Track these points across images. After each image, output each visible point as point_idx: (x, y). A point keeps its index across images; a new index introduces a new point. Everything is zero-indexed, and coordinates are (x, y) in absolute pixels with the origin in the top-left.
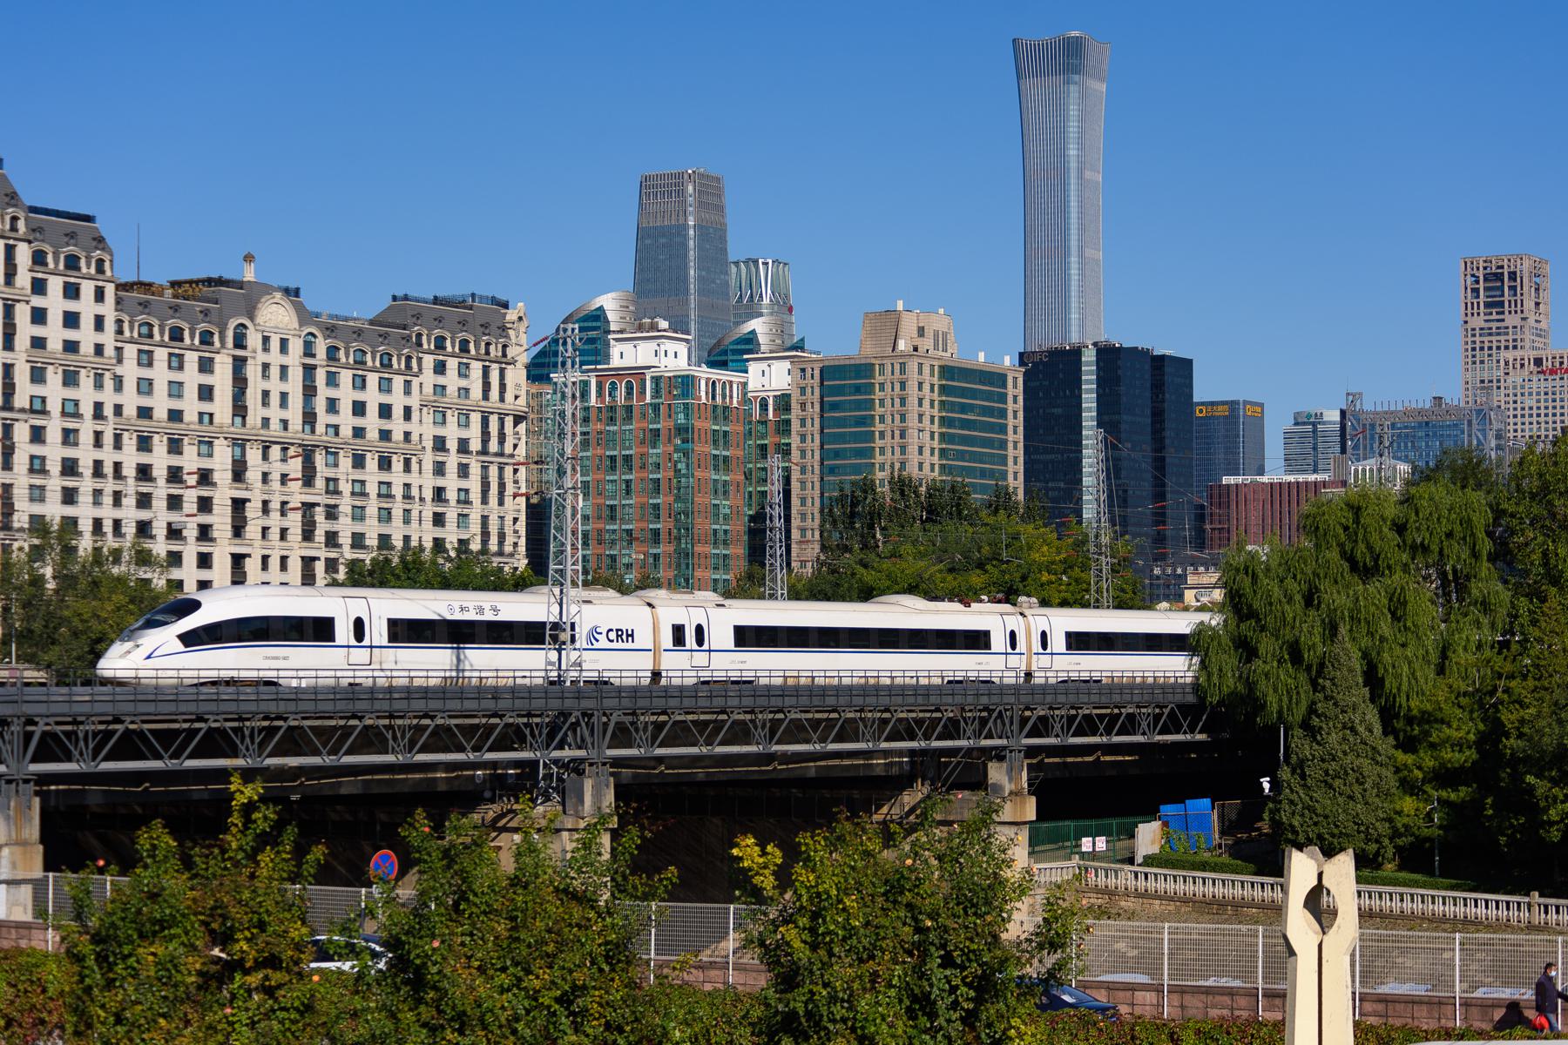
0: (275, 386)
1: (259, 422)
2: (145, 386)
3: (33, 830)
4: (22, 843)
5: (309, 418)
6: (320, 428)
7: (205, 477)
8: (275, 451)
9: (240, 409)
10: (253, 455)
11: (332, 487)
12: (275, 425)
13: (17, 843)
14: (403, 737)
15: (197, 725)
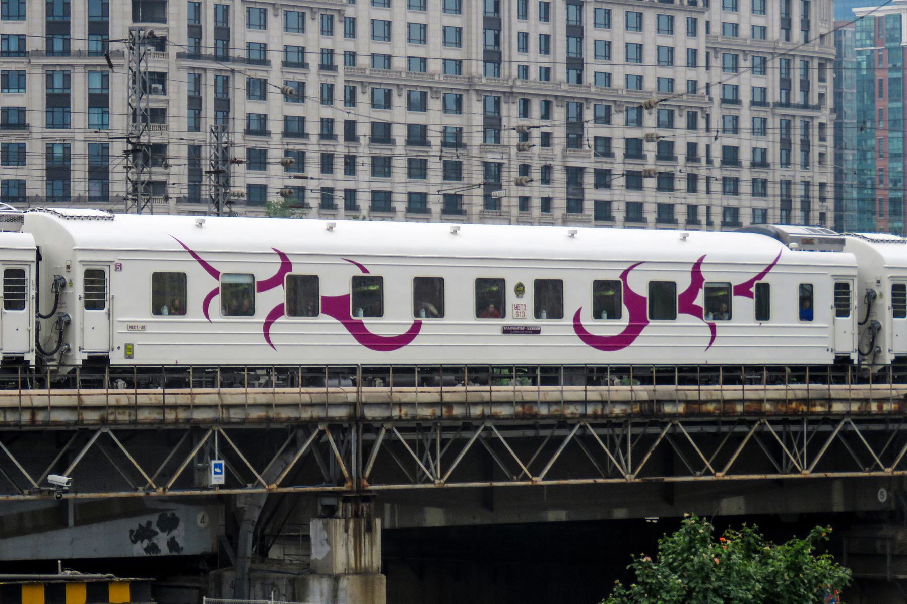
0: (535, 27)
1: (515, 73)
2: (383, 31)
3: (373, 556)
4: (361, 572)
5: (576, 64)
6: (588, 77)
7: (454, 139)
8: (536, 108)
9: (493, 57)
10: (510, 114)
11: (604, 147)
12: (534, 73)
13: (356, 573)
14: (800, 446)
15: (558, 432)
